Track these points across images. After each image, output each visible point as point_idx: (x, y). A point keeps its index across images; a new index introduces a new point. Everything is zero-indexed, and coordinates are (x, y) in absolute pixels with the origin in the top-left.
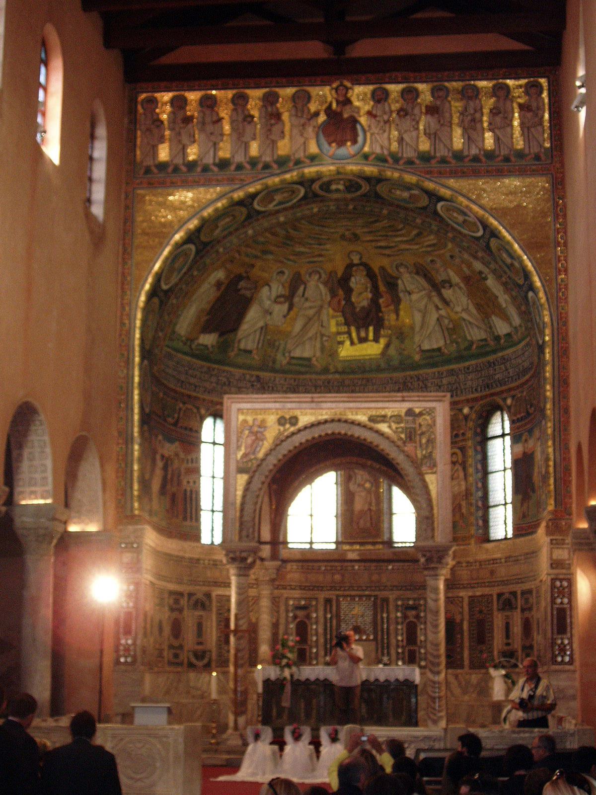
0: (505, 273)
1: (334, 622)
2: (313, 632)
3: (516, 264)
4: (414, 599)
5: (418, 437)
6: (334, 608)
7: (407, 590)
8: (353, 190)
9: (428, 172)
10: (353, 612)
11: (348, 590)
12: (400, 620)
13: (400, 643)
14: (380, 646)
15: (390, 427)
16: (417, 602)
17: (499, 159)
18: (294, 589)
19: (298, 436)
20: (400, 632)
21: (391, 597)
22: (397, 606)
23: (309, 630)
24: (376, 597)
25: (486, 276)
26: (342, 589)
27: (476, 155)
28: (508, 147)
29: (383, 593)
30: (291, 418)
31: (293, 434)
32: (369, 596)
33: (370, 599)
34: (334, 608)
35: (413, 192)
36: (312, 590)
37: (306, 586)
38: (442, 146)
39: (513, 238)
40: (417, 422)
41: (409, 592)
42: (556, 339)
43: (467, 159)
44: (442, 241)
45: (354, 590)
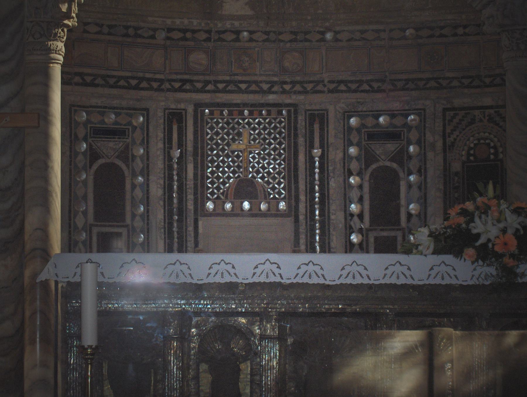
1: (190, 168)
2: (139, 193)
4: (393, 116)
6: (190, 136)
7: (373, 91)
10: (234, 147)
11: (224, 91)
12: (354, 166)
13: (356, 223)
14: (302, 229)
16: (398, 121)
18: (93, 84)
20: (355, 194)
21: (331, 108)
22: (350, 129)
23: (128, 186)
24: (295, 105)
26: (210, 87)
29: (316, 98)
32: (278, 105)
33: (280, 113)
34: (190, 136)
36: (137, 88)
37: (120, 78)
41: (379, 96)
45: (240, 91)
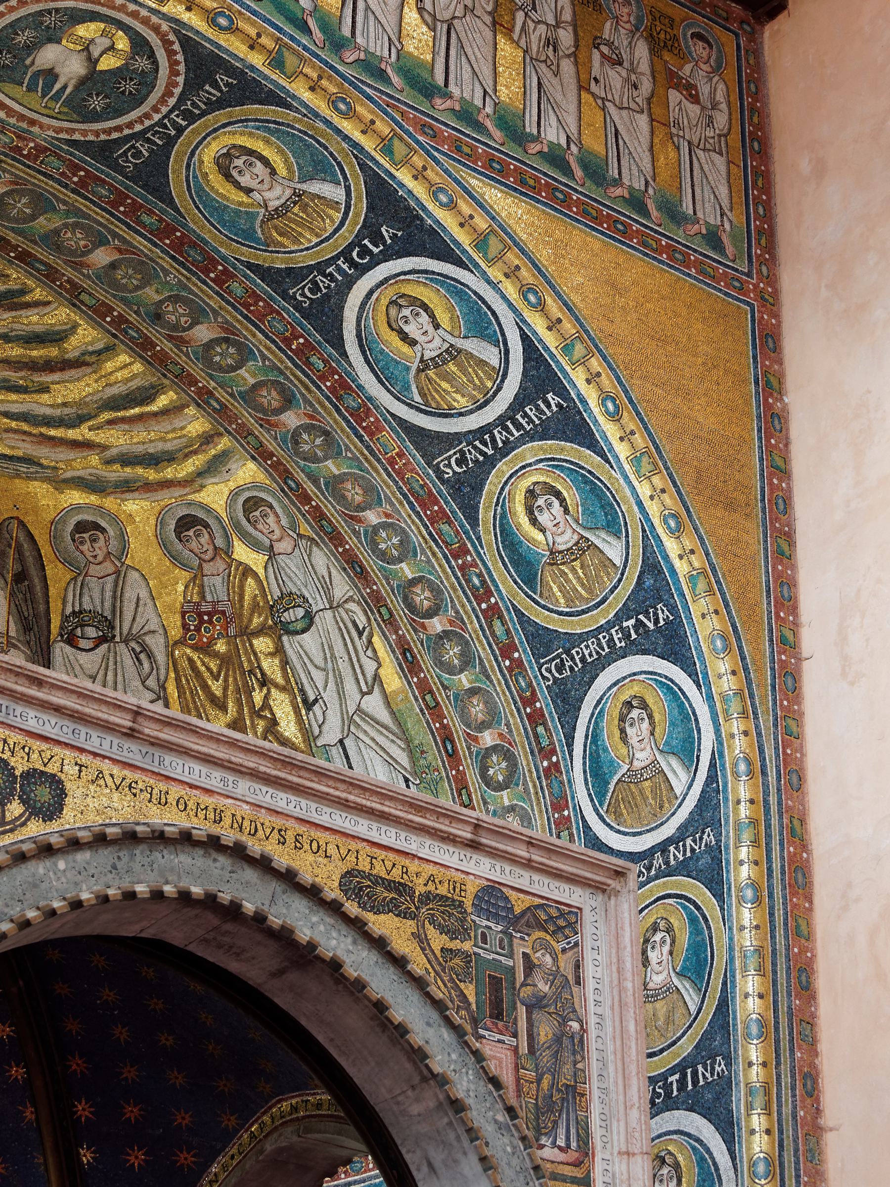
0: (483, 593)
3: (614, 551)
5: (522, 1011)
8: (96, 103)
9: (423, 128)
15: (421, 939)
17: (618, 192)
19: (62, 865)
25: (309, 618)
27: (559, 145)
28: (640, 171)
30: (31, 775)
31: (46, 850)
35: (315, 187)
38: (466, 66)
39: (657, 448)
40: (520, 949)
42: (774, 821)
43: (534, 148)
44: (224, 443)
